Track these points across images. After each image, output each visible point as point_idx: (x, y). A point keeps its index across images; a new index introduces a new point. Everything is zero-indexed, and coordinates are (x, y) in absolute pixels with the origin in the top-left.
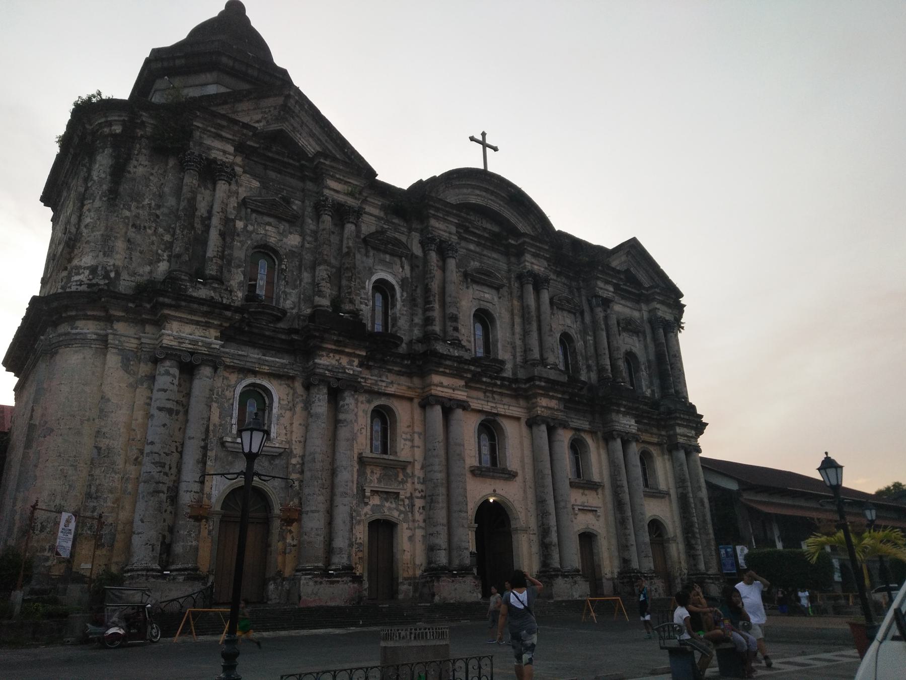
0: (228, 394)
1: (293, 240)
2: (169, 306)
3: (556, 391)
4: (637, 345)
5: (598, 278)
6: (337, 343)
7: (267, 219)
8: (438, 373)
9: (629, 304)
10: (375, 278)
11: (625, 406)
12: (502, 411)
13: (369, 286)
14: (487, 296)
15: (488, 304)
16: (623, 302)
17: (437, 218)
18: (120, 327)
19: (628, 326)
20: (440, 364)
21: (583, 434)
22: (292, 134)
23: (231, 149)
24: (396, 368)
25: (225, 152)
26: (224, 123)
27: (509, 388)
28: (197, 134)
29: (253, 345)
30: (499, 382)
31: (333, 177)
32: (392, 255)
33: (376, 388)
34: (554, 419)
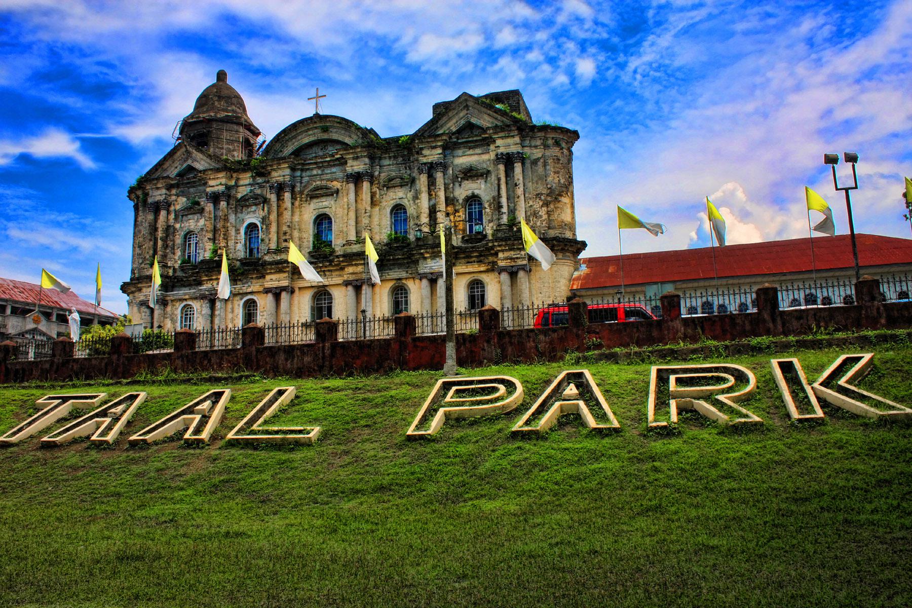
0: (175, 312)
1: (202, 222)
2: (138, 283)
3: (356, 260)
4: (483, 186)
5: (422, 149)
6: (206, 276)
7: (190, 216)
8: (268, 274)
9: (478, 151)
10: (246, 224)
11: (427, 253)
12: (327, 283)
13: (242, 231)
14: (324, 203)
15: (325, 209)
16: (471, 152)
17: (274, 170)
18: (136, 294)
19: (470, 173)
20: (266, 270)
21: (404, 281)
22: (192, 165)
23: (164, 191)
24: (254, 276)
25: (161, 195)
26: (155, 182)
27: (330, 265)
28: (150, 193)
29: (185, 286)
30: (321, 265)
31: (210, 179)
32: (256, 205)
33: (241, 292)
34: (357, 280)
